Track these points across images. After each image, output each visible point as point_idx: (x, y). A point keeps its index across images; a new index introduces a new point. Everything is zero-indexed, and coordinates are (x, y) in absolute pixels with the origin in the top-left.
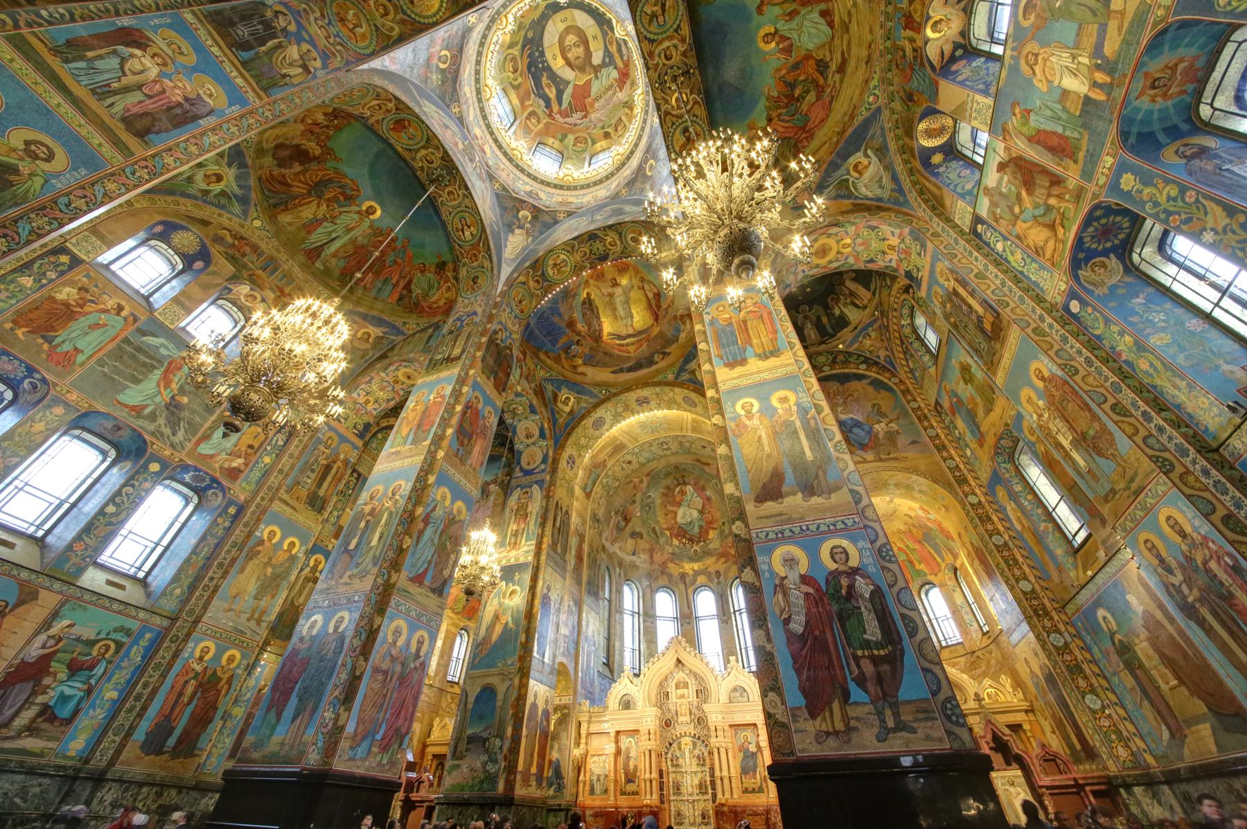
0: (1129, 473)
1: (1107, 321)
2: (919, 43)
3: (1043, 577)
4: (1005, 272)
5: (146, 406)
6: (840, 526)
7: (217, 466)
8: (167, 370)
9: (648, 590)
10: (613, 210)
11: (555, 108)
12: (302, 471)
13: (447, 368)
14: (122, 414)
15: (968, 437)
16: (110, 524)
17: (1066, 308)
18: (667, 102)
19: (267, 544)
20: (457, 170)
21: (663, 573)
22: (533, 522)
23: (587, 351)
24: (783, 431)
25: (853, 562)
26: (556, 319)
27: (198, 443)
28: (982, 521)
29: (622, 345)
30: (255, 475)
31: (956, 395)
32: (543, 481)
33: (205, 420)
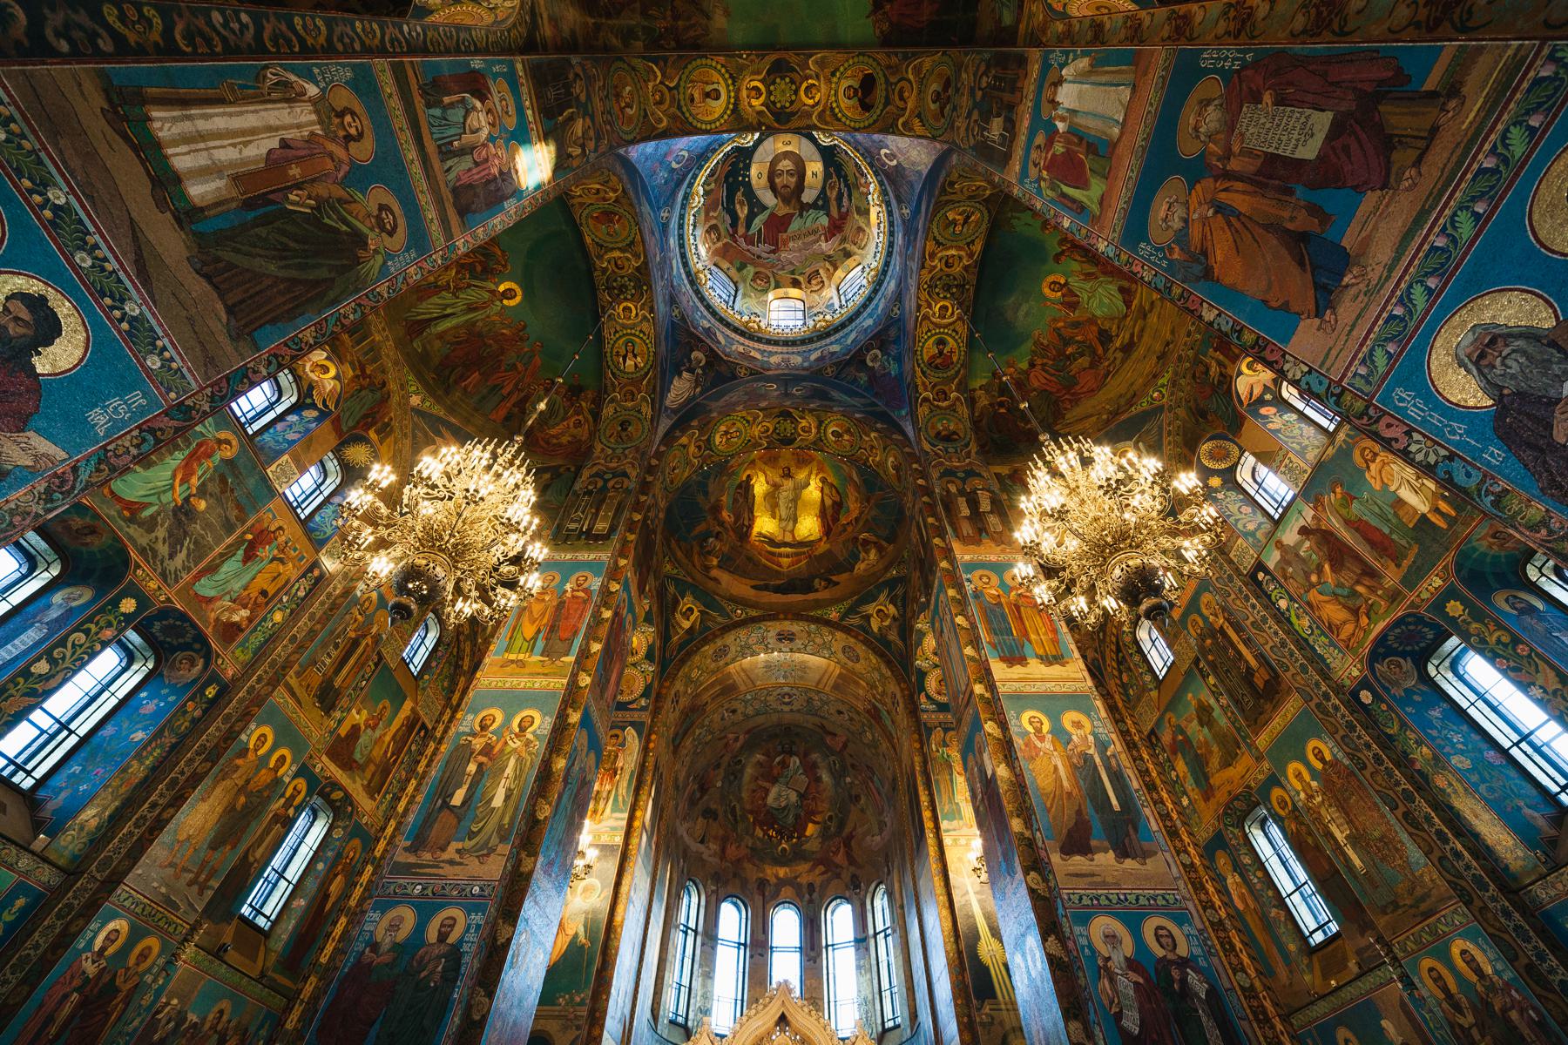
0: (1419, 891)
1: (1403, 725)
2: (1229, 371)
3: (1266, 972)
4: (1287, 633)
5: (146, 506)
6: (1161, 902)
7: (213, 615)
8: (191, 455)
9: (714, 898)
10: (815, 389)
11: (741, 230)
12: (324, 645)
13: (589, 548)
14: (109, 512)
15: (1190, 784)
16: (32, 693)
17: (1355, 694)
18: (930, 306)
19: (251, 756)
20: (650, 287)
21: (735, 875)
22: (624, 784)
23: (726, 549)
24: (1084, 768)
25: (1183, 951)
26: (700, 498)
27: (197, 578)
28: (1195, 889)
29: (773, 554)
30: (257, 639)
31: (1183, 732)
32: (642, 724)
33: (218, 541)
